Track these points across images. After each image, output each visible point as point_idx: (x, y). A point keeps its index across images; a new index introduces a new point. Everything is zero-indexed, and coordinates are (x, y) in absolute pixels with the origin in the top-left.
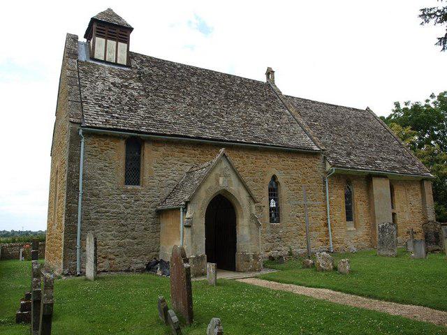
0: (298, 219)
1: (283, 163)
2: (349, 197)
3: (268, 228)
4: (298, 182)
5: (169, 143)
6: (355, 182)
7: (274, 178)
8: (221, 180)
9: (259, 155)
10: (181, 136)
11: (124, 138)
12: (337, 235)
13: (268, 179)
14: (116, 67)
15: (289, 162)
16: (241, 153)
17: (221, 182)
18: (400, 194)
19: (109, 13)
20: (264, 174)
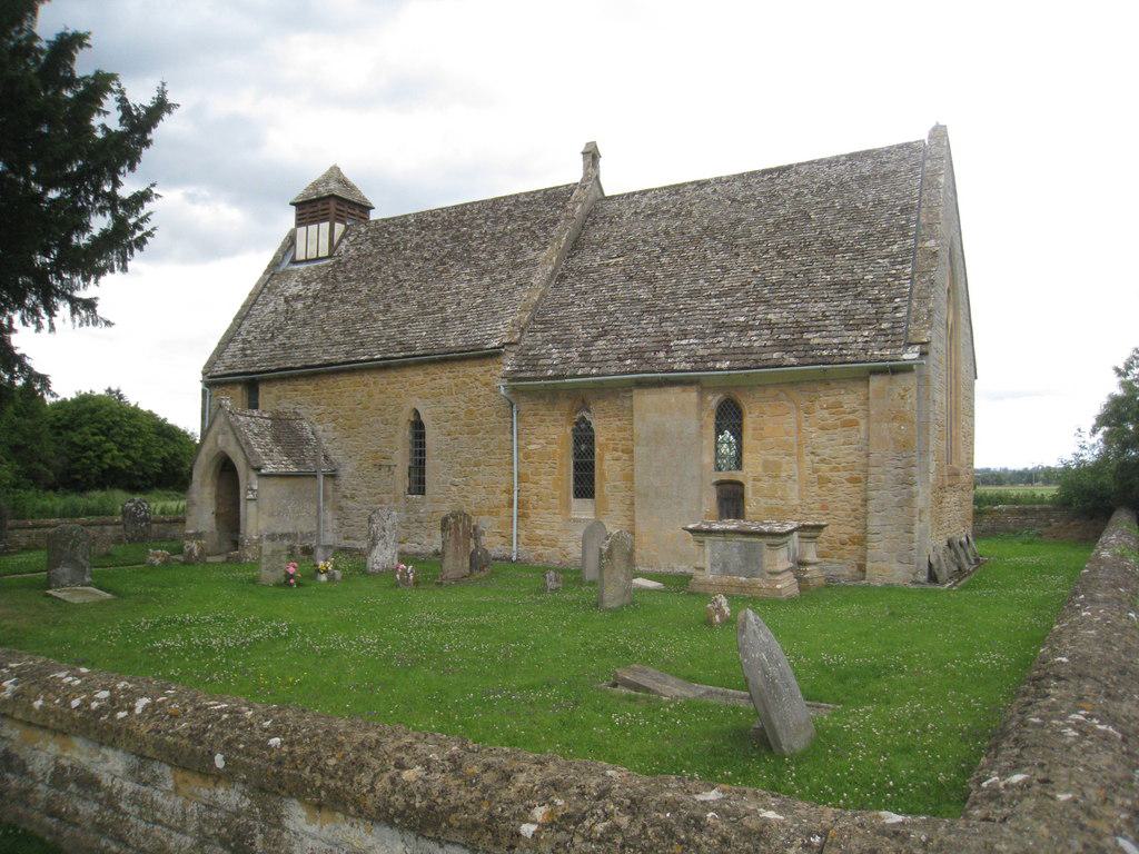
0: (454, 488)
1: (433, 384)
2: (584, 440)
3: (402, 500)
4: (457, 418)
5: (282, 379)
6: (601, 404)
7: (416, 413)
8: (220, 438)
9: (392, 375)
10: (291, 368)
11: (240, 382)
12: (541, 527)
13: (405, 417)
14: (312, 265)
15: (444, 377)
16: (367, 378)
17: (219, 442)
18: (768, 423)
19: (335, 174)
20: (399, 408)
